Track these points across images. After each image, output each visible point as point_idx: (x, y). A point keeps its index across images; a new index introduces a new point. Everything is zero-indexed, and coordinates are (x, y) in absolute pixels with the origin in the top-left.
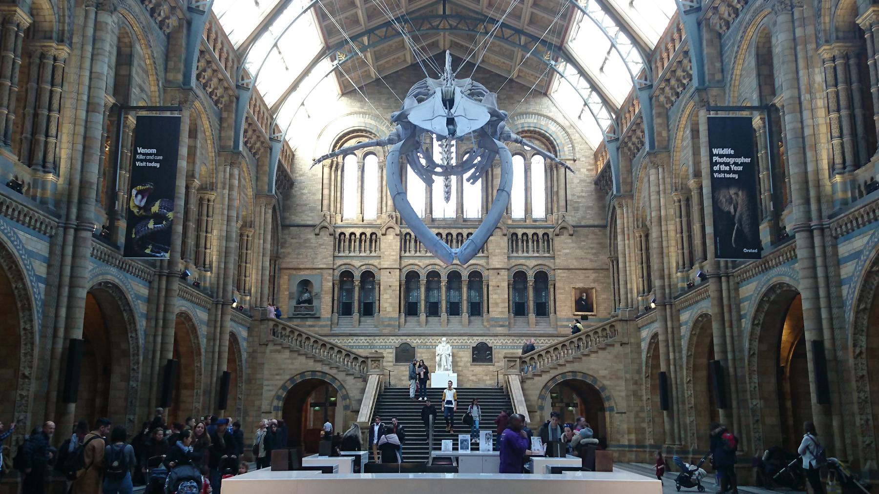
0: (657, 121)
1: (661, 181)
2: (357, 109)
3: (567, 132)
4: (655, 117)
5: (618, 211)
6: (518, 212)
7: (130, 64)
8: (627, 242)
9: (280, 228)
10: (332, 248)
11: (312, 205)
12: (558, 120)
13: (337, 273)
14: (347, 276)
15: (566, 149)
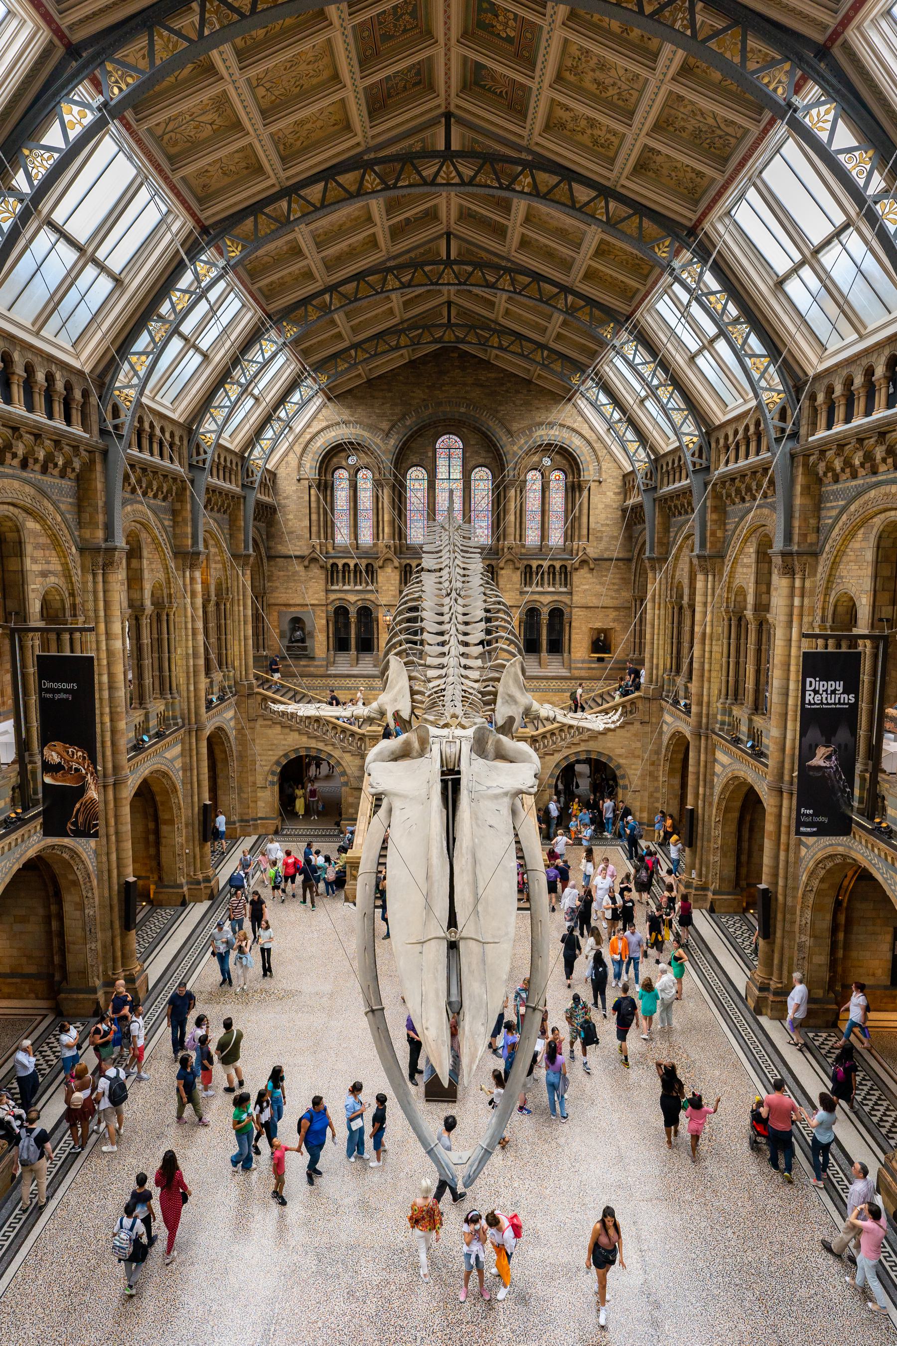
0: (710, 516)
1: (710, 591)
2: (345, 418)
3: (593, 448)
4: (709, 510)
5: (650, 575)
6: (532, 537)
7: (21, 554)
8: (657, 612)
9: (265, 560)
10: (323, 582)
11: (299, 532)
12: (584, 432)
13: (331, 609)
14: (341, 612)
15: (591, 468)
